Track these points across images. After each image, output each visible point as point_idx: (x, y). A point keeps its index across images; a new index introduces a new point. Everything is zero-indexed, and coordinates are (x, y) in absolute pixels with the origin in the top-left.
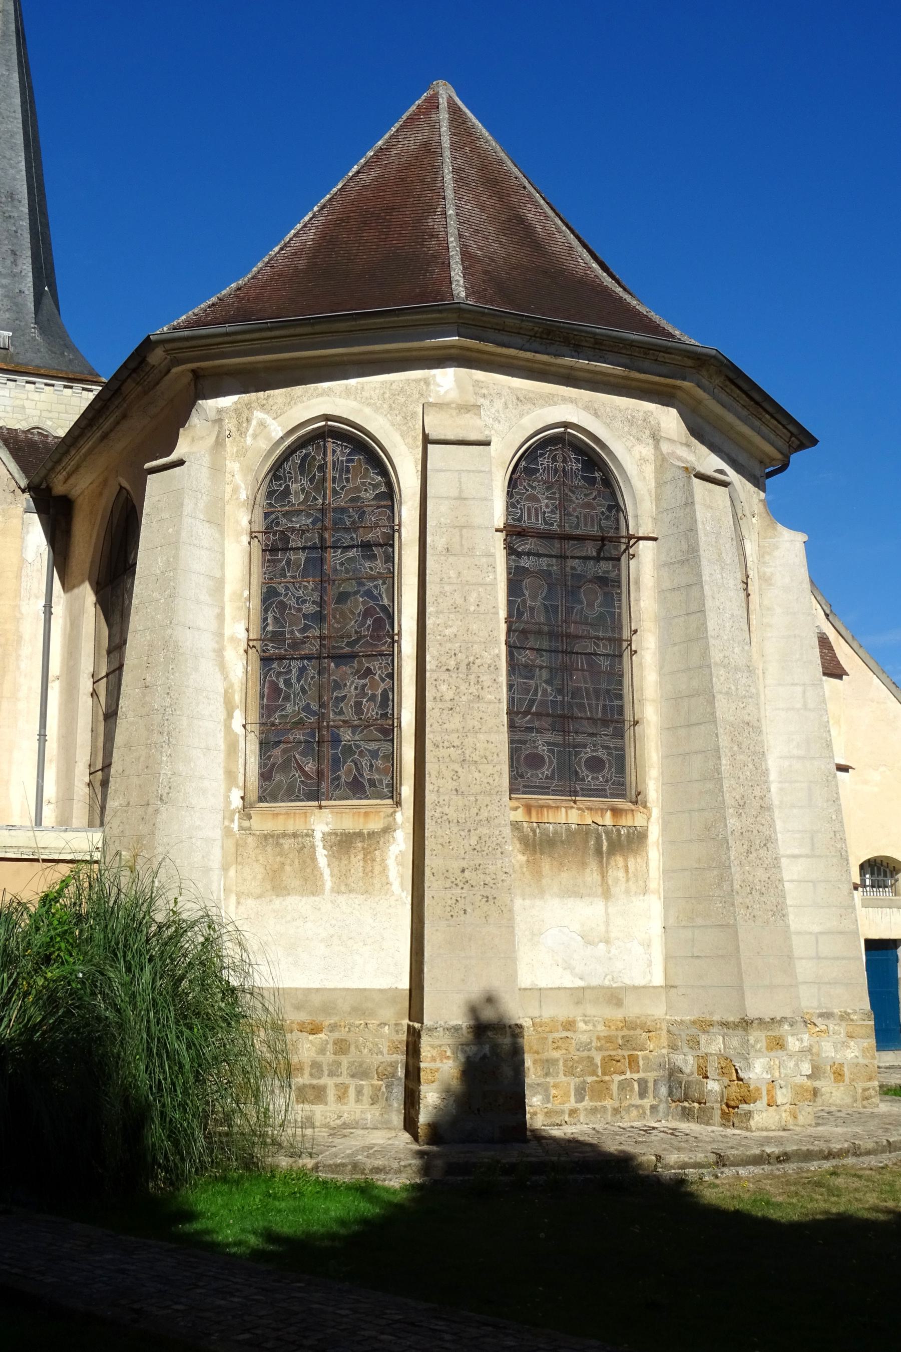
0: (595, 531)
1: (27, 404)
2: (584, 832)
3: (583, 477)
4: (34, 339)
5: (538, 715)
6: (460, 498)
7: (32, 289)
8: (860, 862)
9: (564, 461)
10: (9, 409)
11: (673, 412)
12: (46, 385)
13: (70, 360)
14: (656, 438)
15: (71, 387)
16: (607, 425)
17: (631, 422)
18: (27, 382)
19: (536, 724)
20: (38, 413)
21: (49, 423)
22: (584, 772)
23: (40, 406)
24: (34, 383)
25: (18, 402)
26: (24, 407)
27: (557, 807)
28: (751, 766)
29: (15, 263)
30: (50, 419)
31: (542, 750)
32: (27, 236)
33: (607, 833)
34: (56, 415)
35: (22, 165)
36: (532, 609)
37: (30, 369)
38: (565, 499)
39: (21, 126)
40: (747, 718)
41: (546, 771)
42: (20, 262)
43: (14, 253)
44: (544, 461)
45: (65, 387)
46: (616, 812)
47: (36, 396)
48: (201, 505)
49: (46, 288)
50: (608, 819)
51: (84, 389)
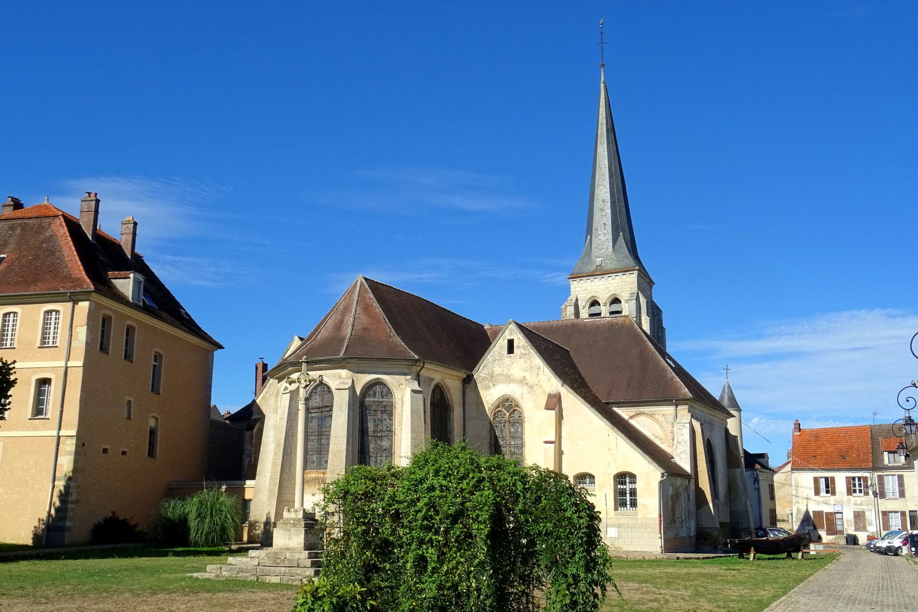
0: (329, 404)
1: (609, 285)
2: (316, 478)
3: (328, 391)
4: (612, 258)
5: (315, 451)
6: (285, 406)
7: (611, 237)
8: (574, 475)
9: (324, 388)
10: (603, 289)
11: (345, 370)
12: (616, 276)
13: (626, 263)
14: (340, 378)
15: (625, 274)
16: (329, 378)
17: (334, 376)
18: (609, 277)
19: (314, 453)
20: (613, 288)
21: (618, 291)
22: (324, 464)
23: (615, 285)
24: (611, 276)
25: (607, 286)
26: (608, 287)
27: (310, 473)
28: (339, 461)
29: (605, 228)
30: (618, 289)
31: (315, 459)
32: (610, 215)
33: (321, 479)
34: (620, 287)
35: (608, 187)
36: (314, 426)
37: (609, 271)
38: (323, 398)
39: (608, 170)
40: (340, 449)
41: (315, 464)
42: (607, 227)
43: (604, 224)
44: (319, 389)
45: (623, 275)
46: (324, 473)
47: (613, 282)
48: (272, 409)
49: (621, 233)
50: (322, 475)
51: (630, 274)
